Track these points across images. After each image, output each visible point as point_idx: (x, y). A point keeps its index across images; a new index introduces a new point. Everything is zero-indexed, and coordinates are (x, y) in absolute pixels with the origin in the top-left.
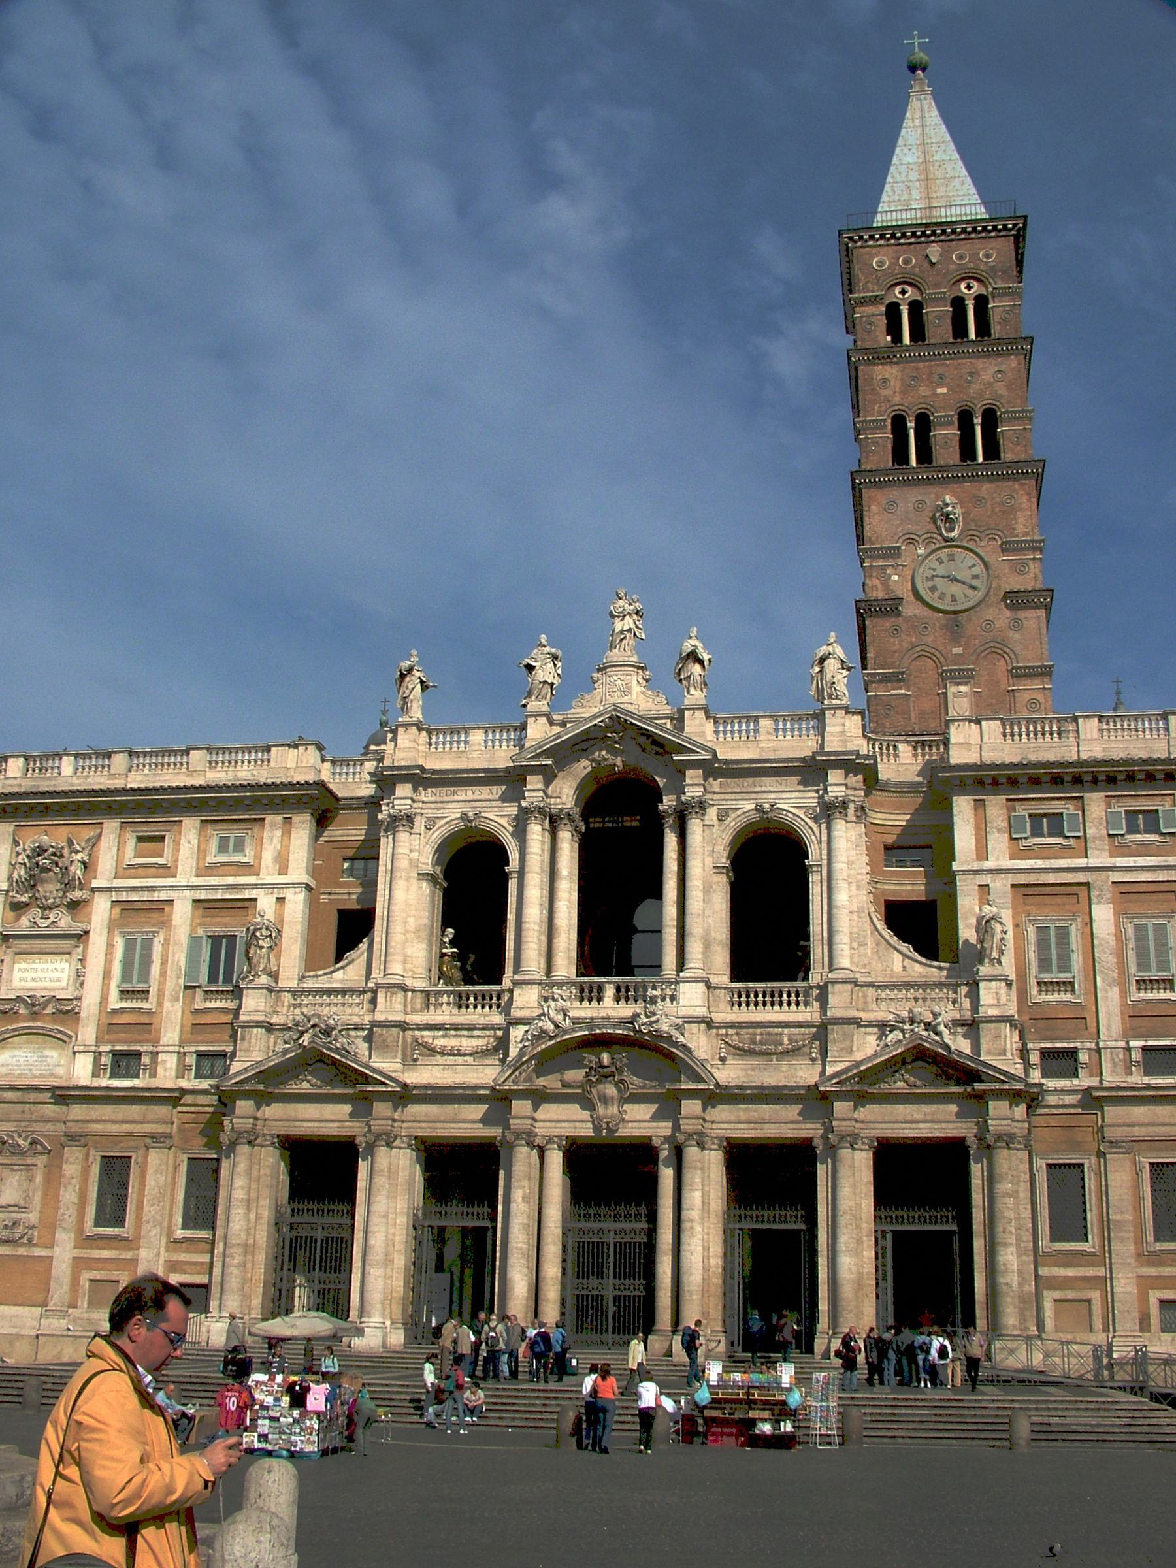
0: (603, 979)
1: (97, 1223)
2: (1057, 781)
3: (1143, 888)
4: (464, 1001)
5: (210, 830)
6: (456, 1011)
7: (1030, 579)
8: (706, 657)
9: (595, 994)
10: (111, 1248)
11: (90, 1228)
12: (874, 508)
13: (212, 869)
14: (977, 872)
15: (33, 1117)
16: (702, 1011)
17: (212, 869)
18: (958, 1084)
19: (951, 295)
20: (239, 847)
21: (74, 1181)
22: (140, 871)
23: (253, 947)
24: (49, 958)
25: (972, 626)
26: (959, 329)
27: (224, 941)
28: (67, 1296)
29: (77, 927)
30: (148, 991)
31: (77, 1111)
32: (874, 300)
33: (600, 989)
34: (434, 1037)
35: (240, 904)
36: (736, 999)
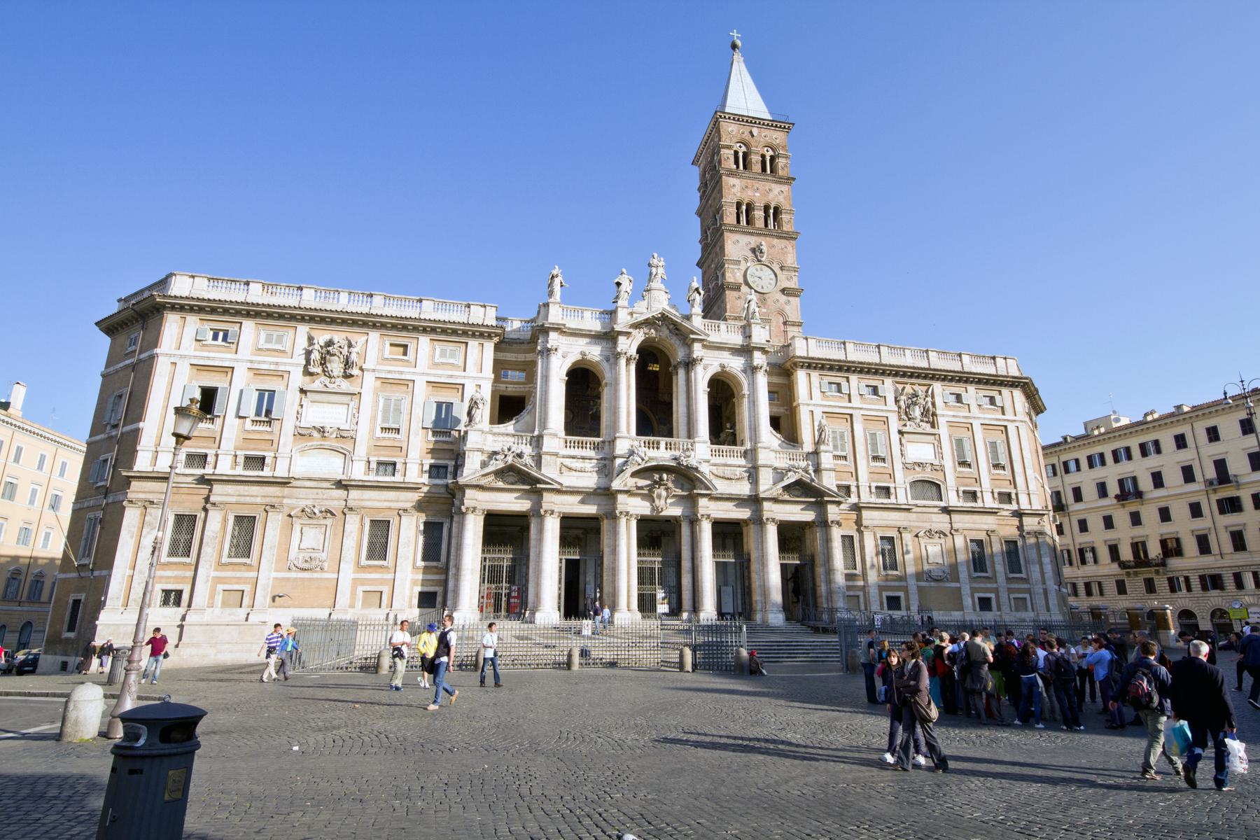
0: (660, 438)
1: (370, 557)
2: (840, 369)
3: (873, 418)
4: (584, 445)
5: (435, 343)
6: (580, 449)
7: (793, 284)
8: (702, 292)
9: (655, 445)
10: (376, 572)
11: (364, 561)
12: (729, 242)
13: (436, 365)
14: (808, 405)
15: (325, 497)
16: (708, 457)
17: (436, 365)
18: (811, 497)
19: (761, 152)
20: (453, 355)
21: (353, 535)
22: (392, 362)
23: (474, 409)
24: (334, 406)
25: (769, 302)
26: (764, 169)
27: (444, 405)
28: (349, 602)
29: (356, 390)
30: (399, 429)
31: (354, 494)
32: (729, 147)
33: (658, 443)
34: (571, 462)
35: (454, 386)
36: (714, 453)
